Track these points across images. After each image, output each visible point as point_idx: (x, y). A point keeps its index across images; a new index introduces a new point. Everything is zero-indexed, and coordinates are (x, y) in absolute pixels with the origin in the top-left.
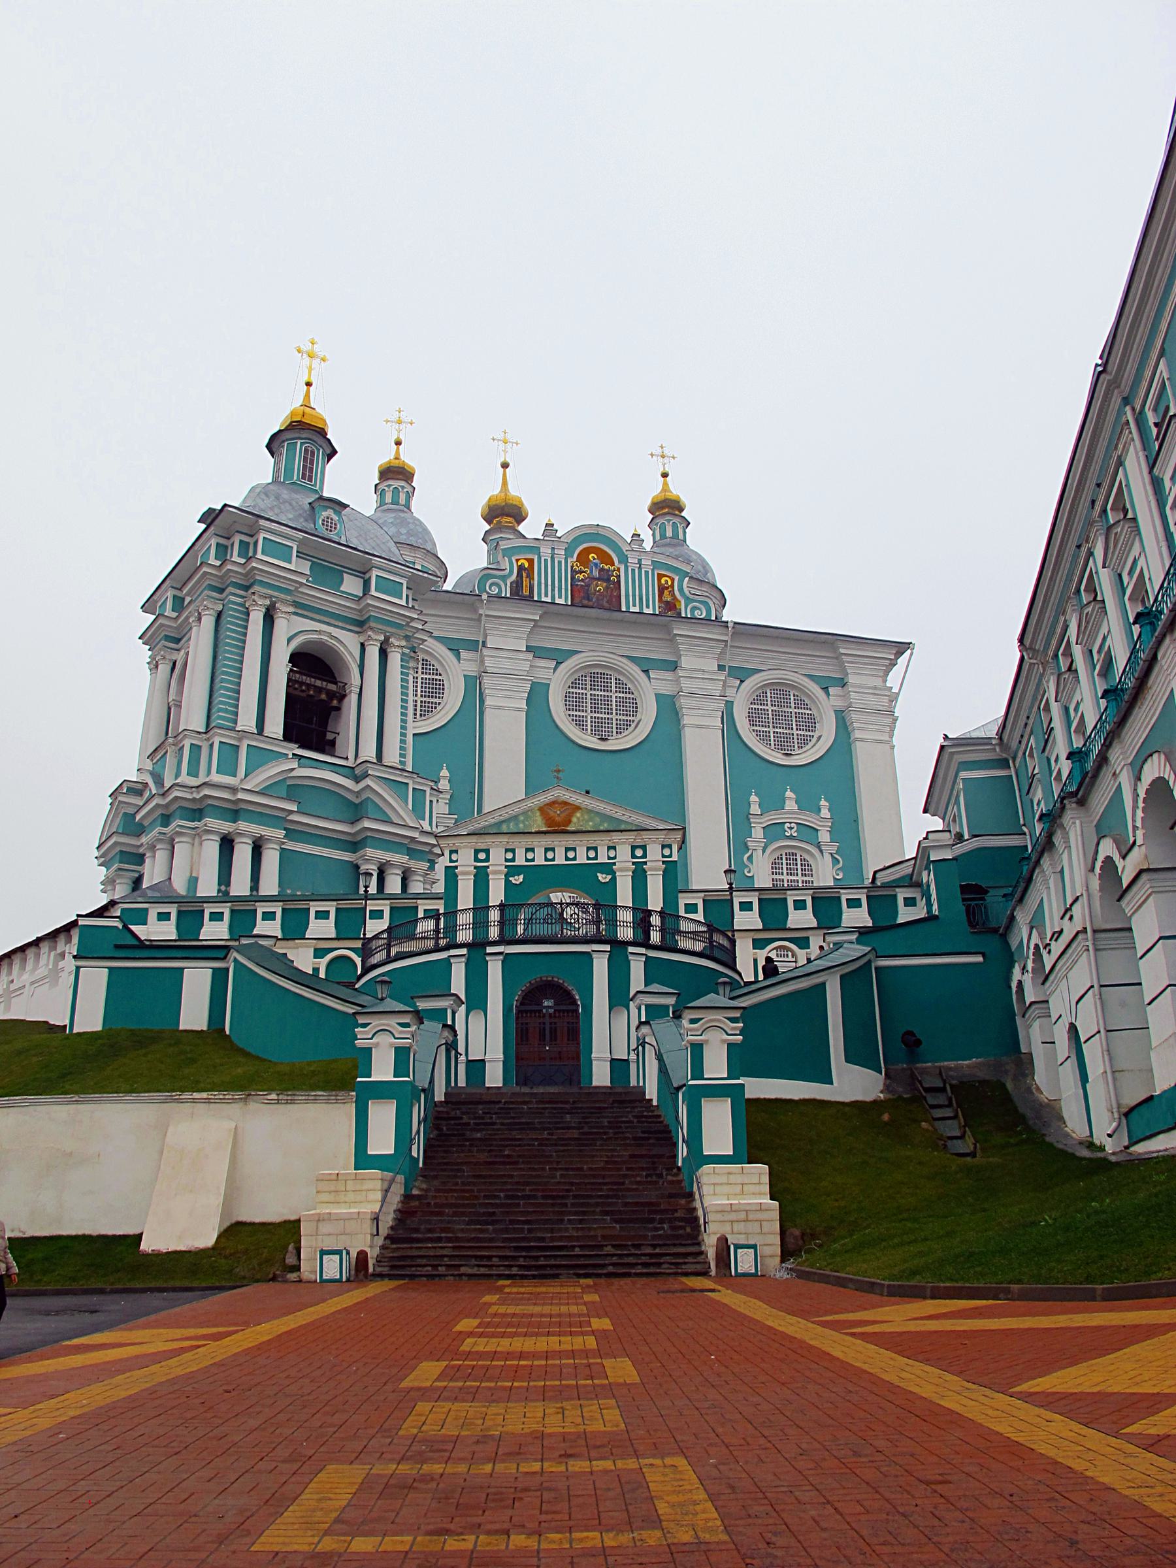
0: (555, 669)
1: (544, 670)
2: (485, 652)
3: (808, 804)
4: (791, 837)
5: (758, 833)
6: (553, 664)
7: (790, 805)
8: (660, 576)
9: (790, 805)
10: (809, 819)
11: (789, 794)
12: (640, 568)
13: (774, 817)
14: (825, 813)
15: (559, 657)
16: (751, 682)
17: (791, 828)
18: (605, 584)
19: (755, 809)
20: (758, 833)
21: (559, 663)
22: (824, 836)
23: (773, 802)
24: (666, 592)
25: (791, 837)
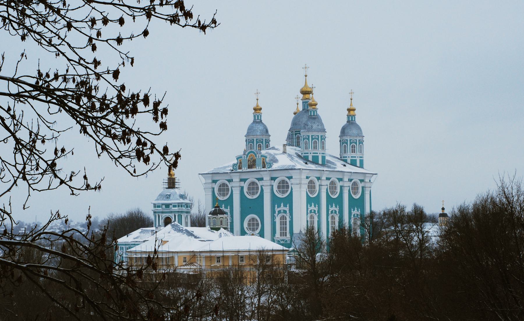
1: (242, 184)
2: (232, 183)
3: (285, 206)
4: (282, 213)
5: (277, 213)
6: (244, 182)
10: (285, 209)
11: (282, 204)
13: (279, 209)
14: (288, 207)
16: (276, 180)
19: (276, 208)
20: (277, 213)
21: (245, 182)
22: (288, 212)
23: (279, 206)
25: (282, 213)
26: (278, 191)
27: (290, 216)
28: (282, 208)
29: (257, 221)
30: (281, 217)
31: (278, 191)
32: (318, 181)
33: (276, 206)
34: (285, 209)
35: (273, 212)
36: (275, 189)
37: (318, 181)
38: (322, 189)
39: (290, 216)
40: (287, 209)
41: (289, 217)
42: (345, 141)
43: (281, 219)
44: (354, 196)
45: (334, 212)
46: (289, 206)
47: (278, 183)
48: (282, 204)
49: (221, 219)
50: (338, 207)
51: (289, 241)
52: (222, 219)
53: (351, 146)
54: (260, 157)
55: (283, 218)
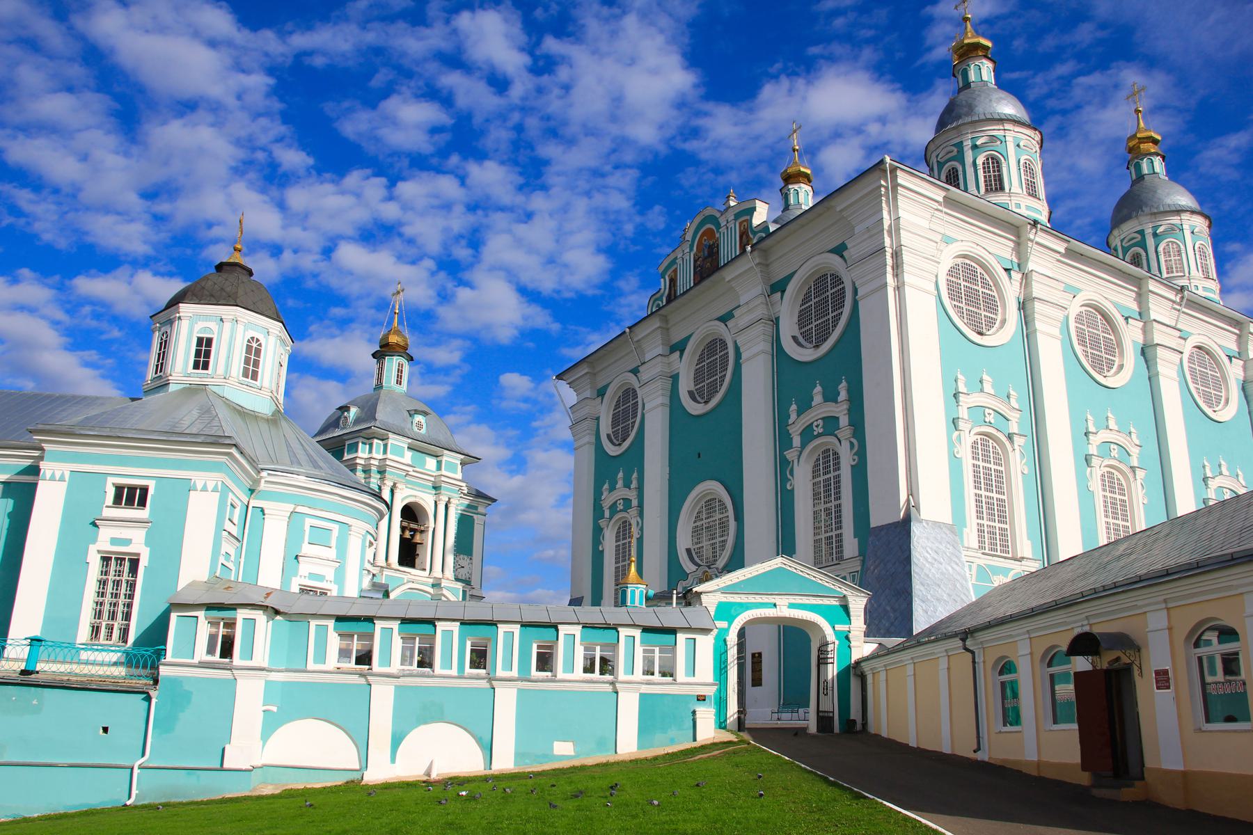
0: (681, 356)
4: (819, 435)
5: (797, 441)
7: (818, 399)
8: (740, 224)
9: (818, 399)
10: (830, 409)
11: (818, 389)
12: (727, 228)
15: (679, 347)
16: (791, 288)
17: (817, 426)
18: (710, 259)
19: (793, 416)
20: (797, 441)
23: (805, 407)
24: (744, 237)
25: (819, 435)
26: (801, 339)
27: (852, 440)
28: (820, 408)
29: (723, 506)
30: (818, 460)
31: (801, 339)
32: (1010, 277)
33: (794, 407)
34: (830, 409)
35: (782, 439)
36: (789, 328)
37: (1010, 277)
38: (1034, 319)
39: (854, 441)
40: (840, 411)
41: (851, 443)
42: (1134, 238)
43: (815, 473)
44: (1209, 411)
45: (1114, 453)
46: (848, 391)
47: (800, 302)
48: (818, 389)
49: (200, 325)
50: (1134, 436)
51: (854, 576)
52: (213, 325)
53: (1161, 249)
54: (731, 225)
55: (828, 461)
